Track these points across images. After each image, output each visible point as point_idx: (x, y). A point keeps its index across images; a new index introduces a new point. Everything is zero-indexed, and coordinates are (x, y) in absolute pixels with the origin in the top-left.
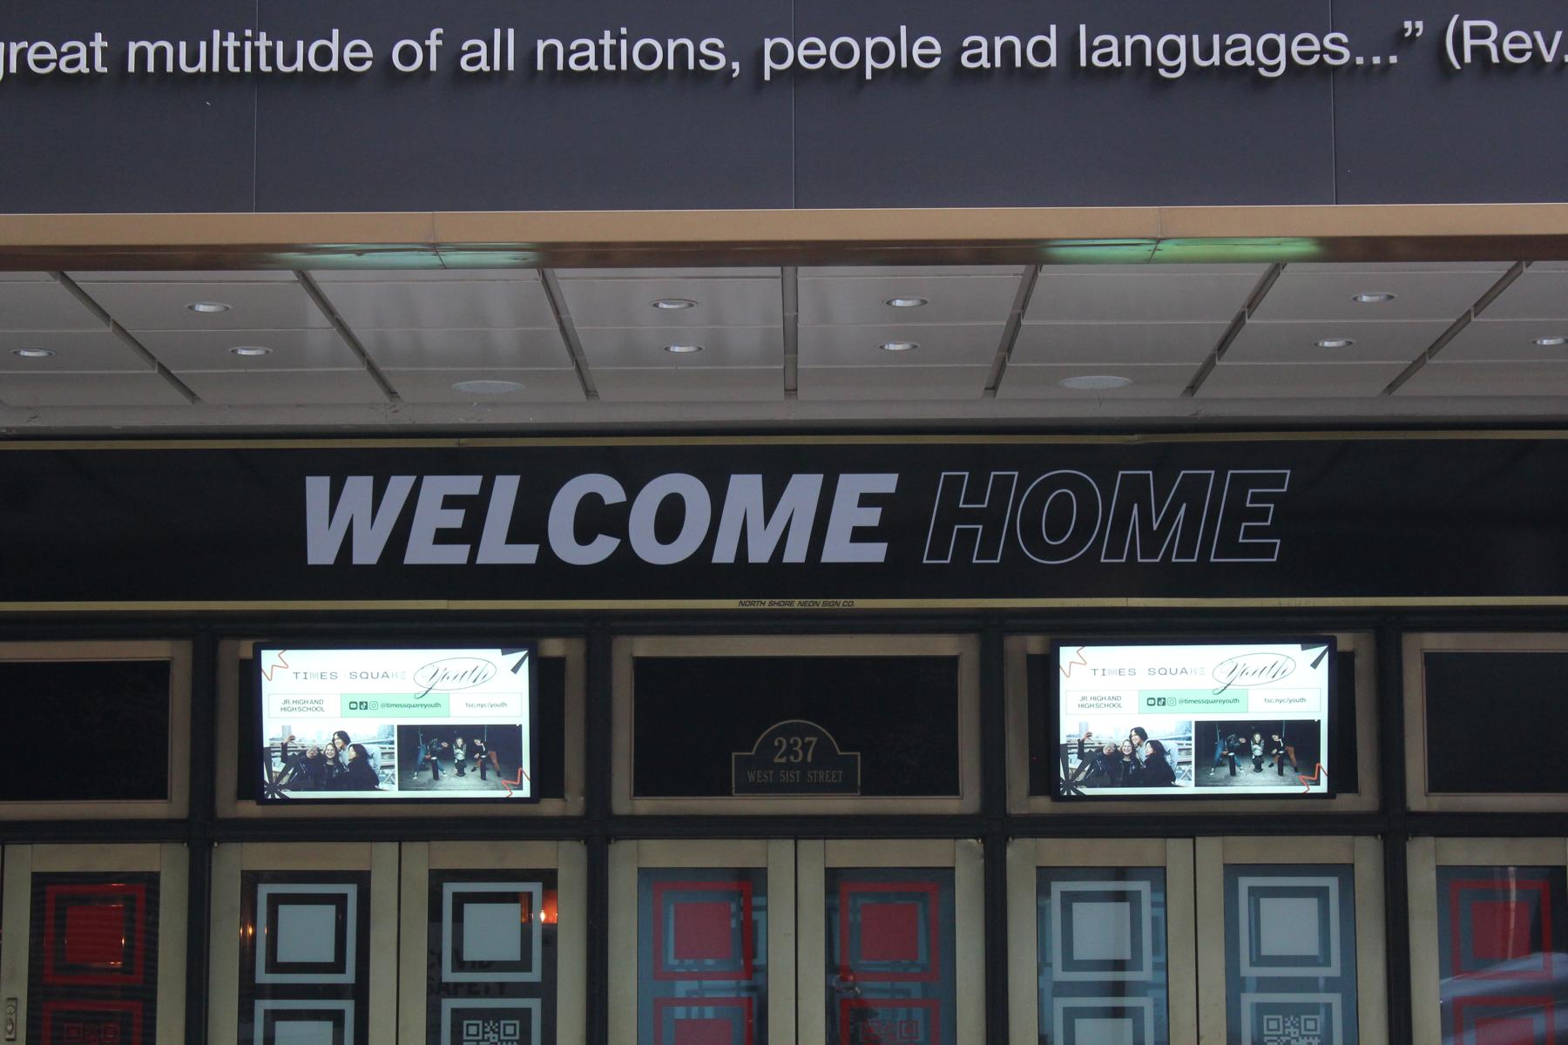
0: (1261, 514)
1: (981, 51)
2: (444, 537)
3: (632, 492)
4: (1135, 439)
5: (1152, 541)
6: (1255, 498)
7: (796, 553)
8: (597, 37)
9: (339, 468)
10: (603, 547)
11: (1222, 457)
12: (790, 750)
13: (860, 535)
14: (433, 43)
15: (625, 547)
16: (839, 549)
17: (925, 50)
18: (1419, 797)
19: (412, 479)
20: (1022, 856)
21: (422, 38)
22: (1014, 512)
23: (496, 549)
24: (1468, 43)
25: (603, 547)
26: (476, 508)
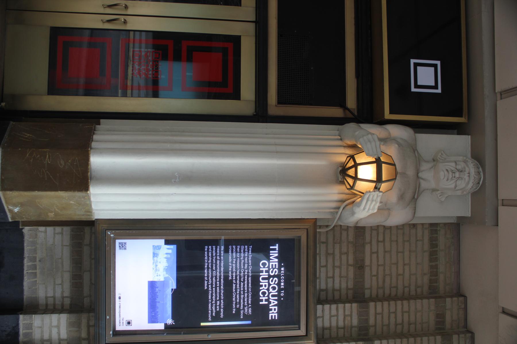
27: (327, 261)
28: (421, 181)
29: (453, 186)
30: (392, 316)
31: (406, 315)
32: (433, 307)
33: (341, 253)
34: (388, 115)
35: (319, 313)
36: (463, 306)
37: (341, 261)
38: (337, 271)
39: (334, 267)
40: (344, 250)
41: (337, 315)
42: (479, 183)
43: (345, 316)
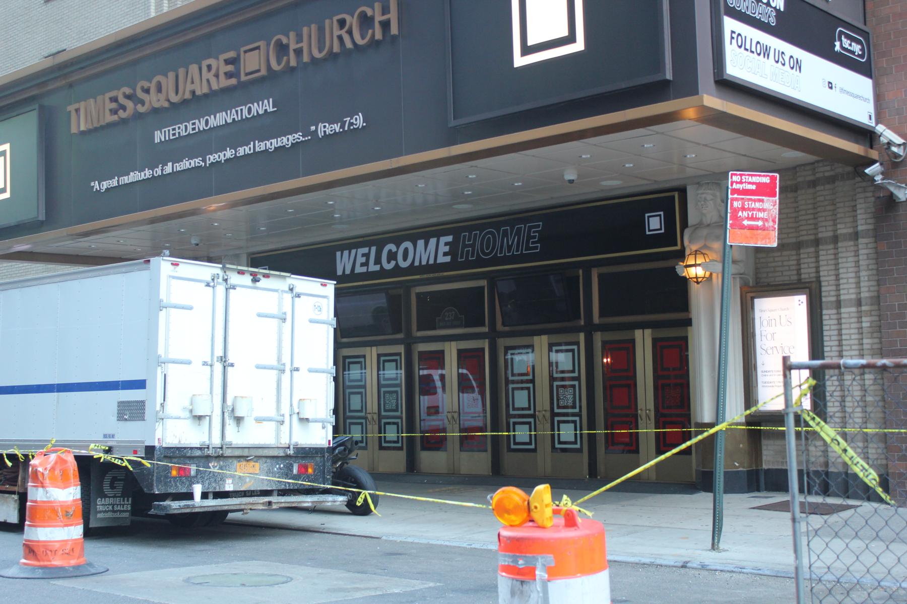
0: (534, 237)
1: (241, 151)
2: (362, 265)
3: (398, 248)
4: (507, 218)
5: (509, 248)
6: (534, 232)
7: (431, 262)
8: (182, 161)
9: (342, 248)
10: (393, 263)
11: (524, 221)
12: (449, 317)
13: (445, 254)
14: (160, 168)
15: (397, 264)
16: (442, 259)
17: (229, 153)
18: (596, 319)
19: (355, 250)
20: (502, 342)
21: (158, 167)
22: (478, 243)
23: (373, 268)
24: (323, 129)
25: (393, 263)
26: (367, 256)
27: (778, 271)
28: (713, 221)
29: (711, 202)
30: (809, 222)
31: (809, 212)
32: (803, 191)
33: (774, 262)
34: (678, 247)
35: (807, 276)
36: (803, 167)
37: (779, 261)
38: (785, 263)
39: (783, 266)
40: (771, 259)
41: (808, 263)
42: (708, 183)
43: (808, 257)
